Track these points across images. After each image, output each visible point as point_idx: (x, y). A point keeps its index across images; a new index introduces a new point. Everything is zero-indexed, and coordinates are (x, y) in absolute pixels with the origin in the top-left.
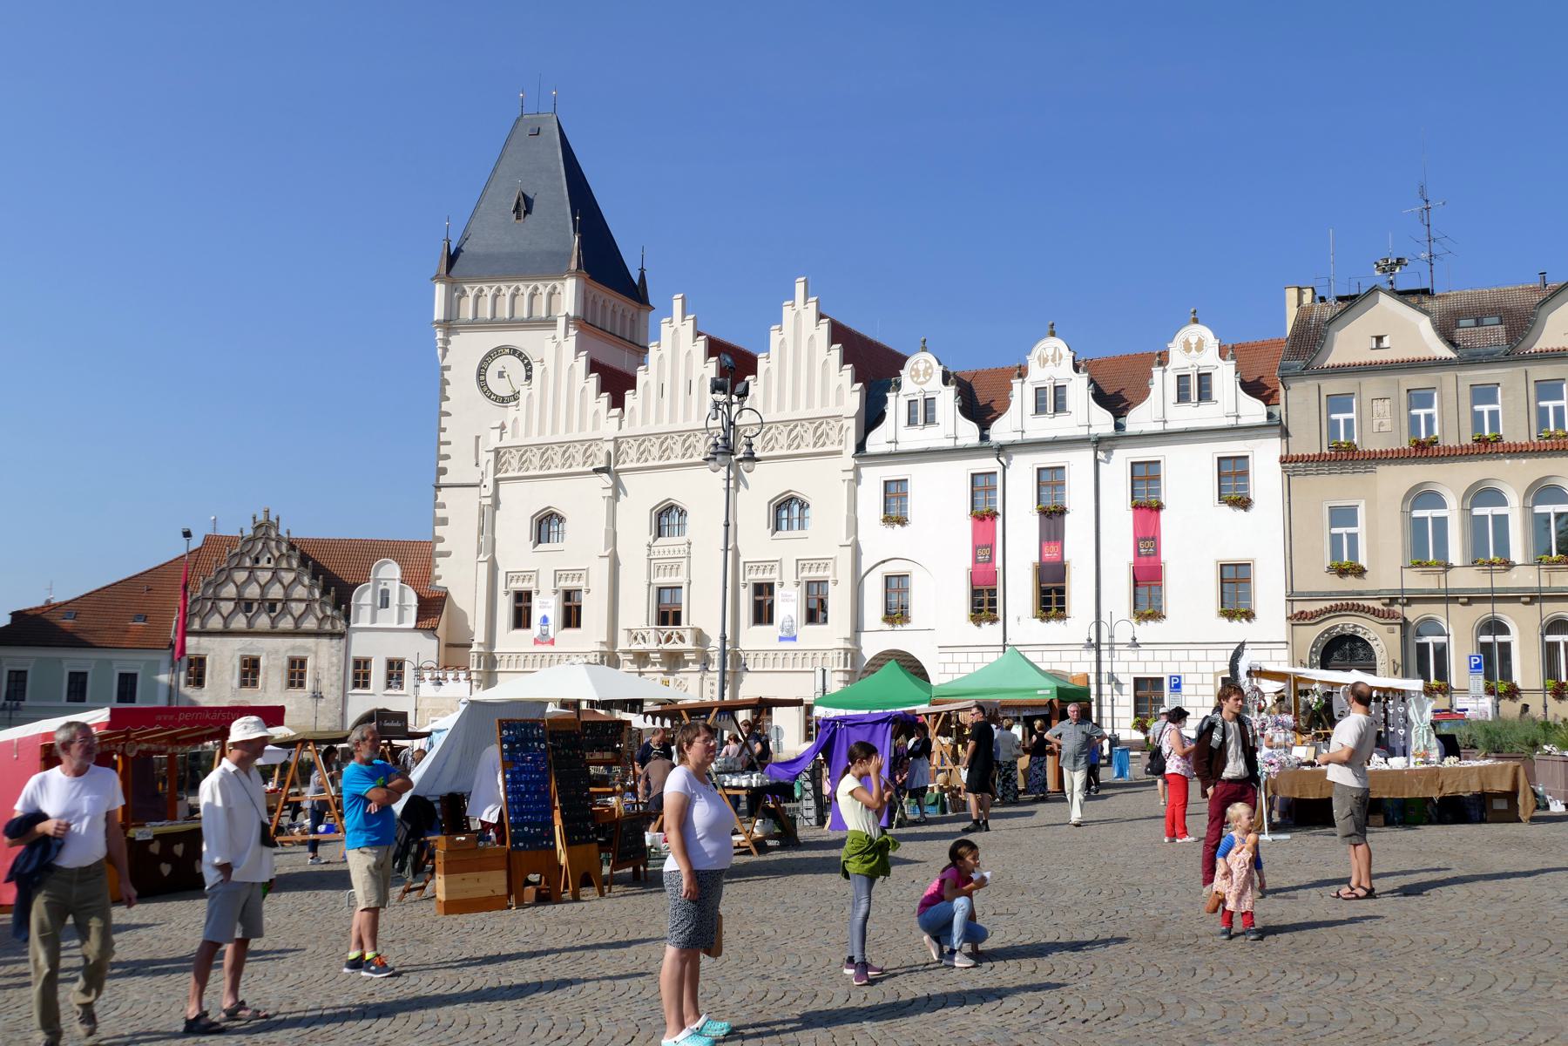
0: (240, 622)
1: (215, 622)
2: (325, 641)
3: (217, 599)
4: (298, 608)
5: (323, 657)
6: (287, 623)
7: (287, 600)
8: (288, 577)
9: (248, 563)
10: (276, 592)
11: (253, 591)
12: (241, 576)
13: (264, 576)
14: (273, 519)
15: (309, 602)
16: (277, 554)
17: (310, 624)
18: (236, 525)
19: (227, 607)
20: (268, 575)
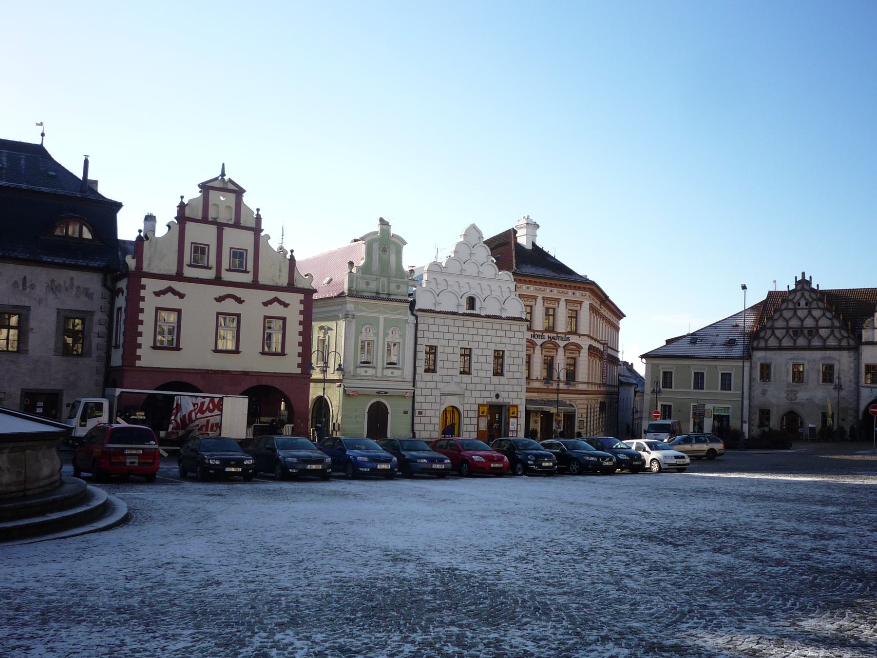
0: (786, 342)
1: (773, 342)
2: (845, 353)
3: (773, 329)
4: (822, 332)
5: (843, 361)
6: (816, 342)
7: (817, 328)
8: (817, 313)
9: (791, 306)
10: (809, 323)
11: (794, 323)
12: (787, 314)
13: (801, 313)
14: (807, 278)
15: (832, 328)
16: (811, 300)
17: (832, 342)
18: (786, 283)
19: (778, 333)
20: (806, 312)
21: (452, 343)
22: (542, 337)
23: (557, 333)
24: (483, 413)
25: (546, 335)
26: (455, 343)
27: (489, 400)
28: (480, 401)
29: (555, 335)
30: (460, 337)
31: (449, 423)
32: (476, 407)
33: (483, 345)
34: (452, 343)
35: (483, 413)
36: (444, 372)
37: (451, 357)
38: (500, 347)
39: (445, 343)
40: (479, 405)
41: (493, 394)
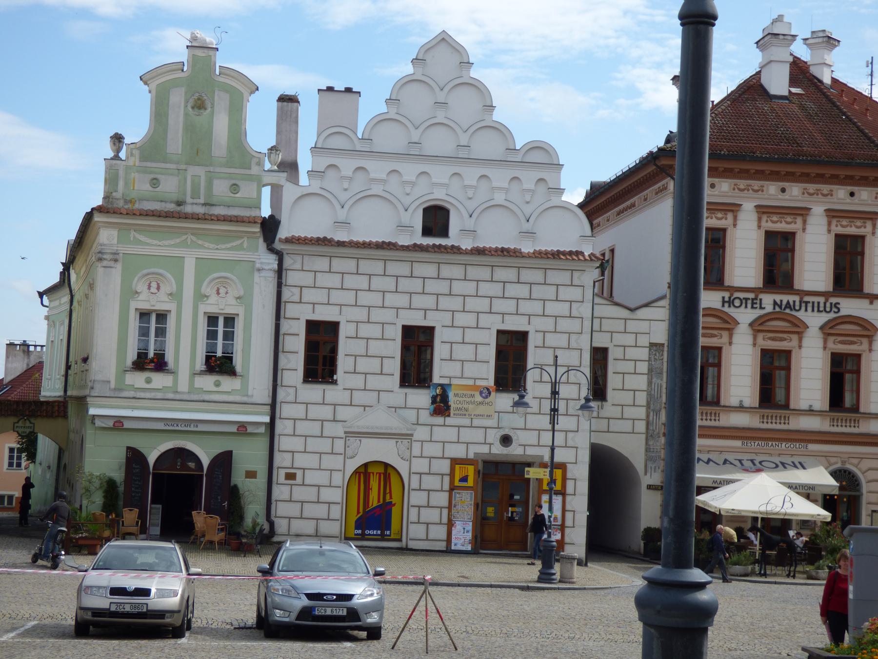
21: (377, 315)
22: (755, 303)
23: (803, 293)
24: (464, 479)
25: (768, 300)
26: (387, 315)
27: (485, 449)
28: (459, 452)
29: (791, 298)
30: (402, 300)
31: (374, 501)
32: (445, 467)
33: (467, 319)
34: (377, 315)
35: (464, 479)
36: (357, 381)
37: (376, 347)
38: (514, 324)
39: (547, 324)
40: (454, 462)
41: (494, 436)
